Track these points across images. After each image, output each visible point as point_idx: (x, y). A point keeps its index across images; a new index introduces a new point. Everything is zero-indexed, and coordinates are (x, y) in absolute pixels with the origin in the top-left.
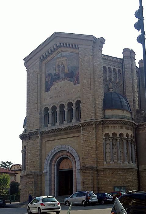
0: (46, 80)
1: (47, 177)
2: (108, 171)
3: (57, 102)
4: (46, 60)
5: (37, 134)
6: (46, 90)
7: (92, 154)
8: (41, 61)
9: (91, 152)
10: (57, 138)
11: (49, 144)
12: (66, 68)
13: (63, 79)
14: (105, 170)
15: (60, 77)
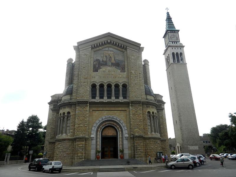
0: (94, 63)
1: (94, 142)
2: (152, 140)
3: (106, 81)
4: (96, 49)
5: (87, 103)
6: (93, 70)
7: (141, 125)
8: (92, 48)
9: (140, 123)
10: (105, 109)
11: (96, 114)
12: (113, 59)
13: (110, 66)
14: (150, 138)
15: (108, 64)
